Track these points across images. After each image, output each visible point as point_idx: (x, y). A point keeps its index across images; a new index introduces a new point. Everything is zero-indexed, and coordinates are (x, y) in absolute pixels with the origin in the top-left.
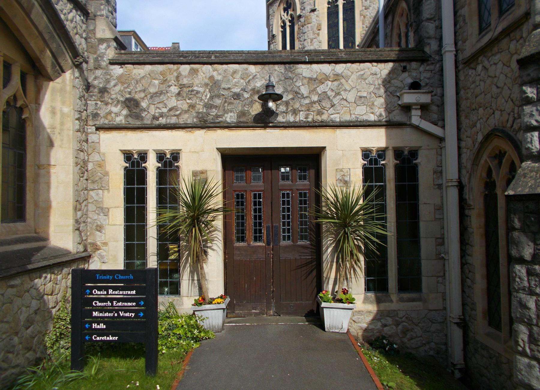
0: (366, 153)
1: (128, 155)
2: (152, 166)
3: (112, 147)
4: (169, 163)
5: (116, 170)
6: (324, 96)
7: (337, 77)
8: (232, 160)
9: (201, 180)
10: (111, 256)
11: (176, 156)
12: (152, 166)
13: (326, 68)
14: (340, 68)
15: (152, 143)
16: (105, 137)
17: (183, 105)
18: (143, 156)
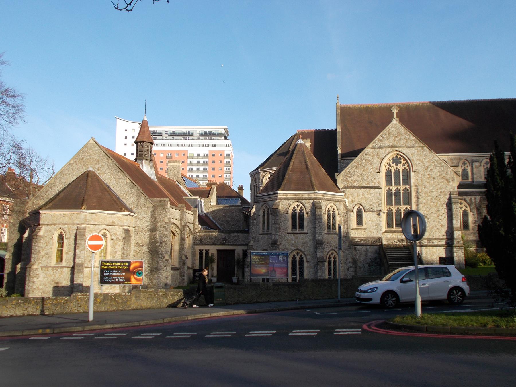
0: (243, 250)
1: (200, 250)
2: (204, 252)
3: (198, 248)
4: (207, 251)
5: (198, 252)
6: (236, 240)
7: (238, 236)
8: (219, 251)
9: (213, 255)
10: (197, 267)
11: (208, 250)
12: (204, 252)
13: (236, 234)
14: (239, 234)
15: (204, 248)
16: (196, 246)
17: (210, 241)
18: (203, 250)
